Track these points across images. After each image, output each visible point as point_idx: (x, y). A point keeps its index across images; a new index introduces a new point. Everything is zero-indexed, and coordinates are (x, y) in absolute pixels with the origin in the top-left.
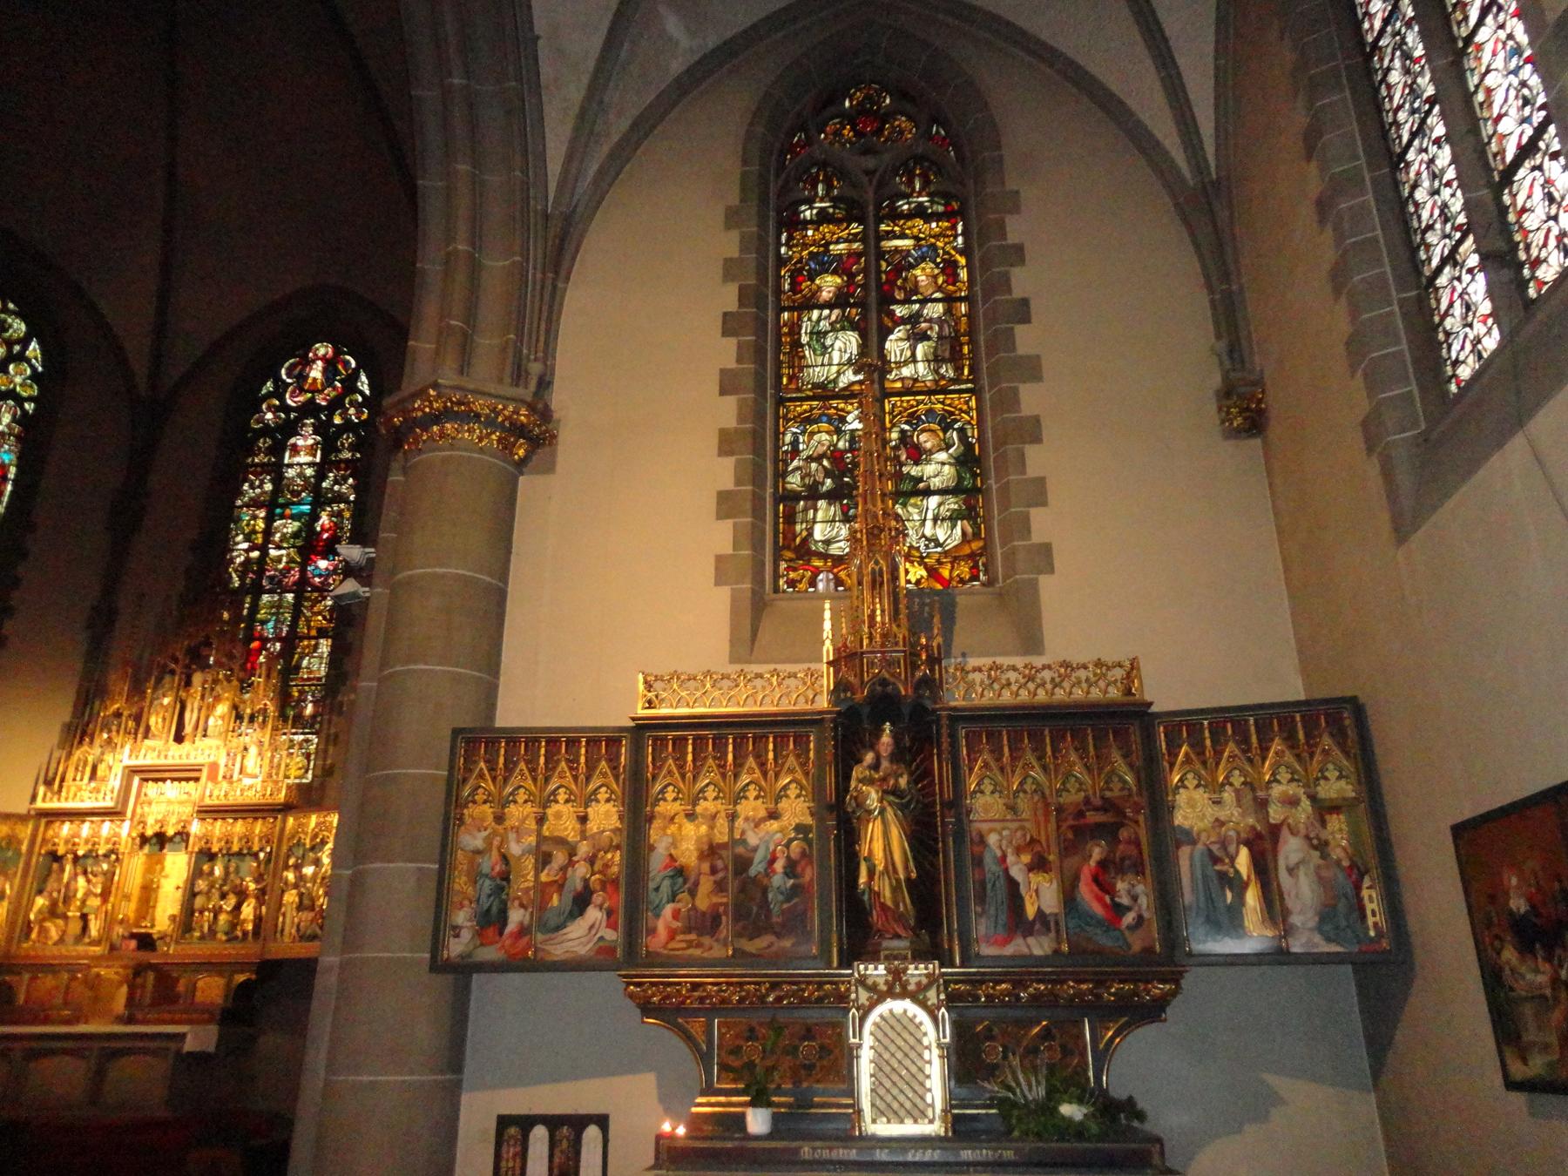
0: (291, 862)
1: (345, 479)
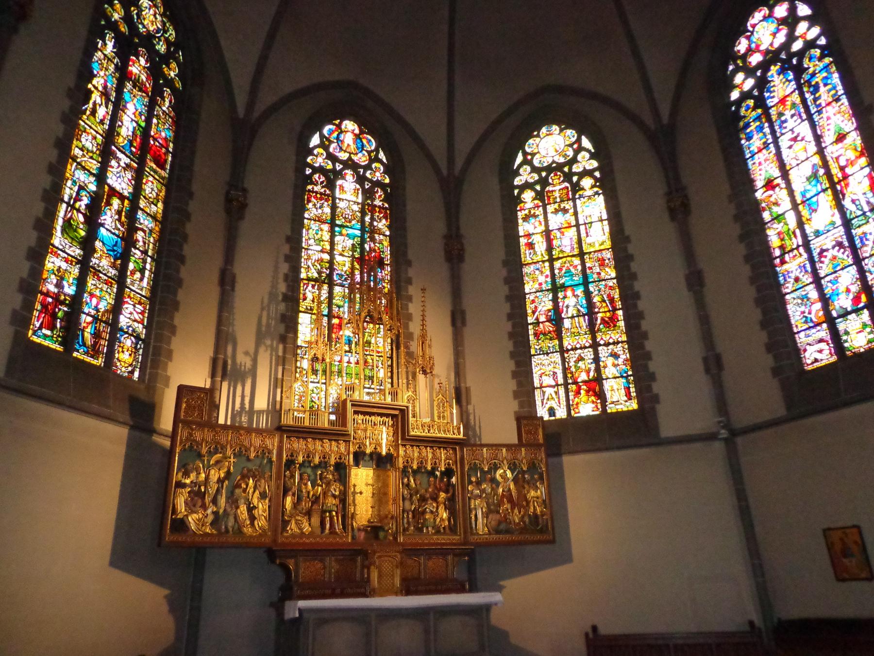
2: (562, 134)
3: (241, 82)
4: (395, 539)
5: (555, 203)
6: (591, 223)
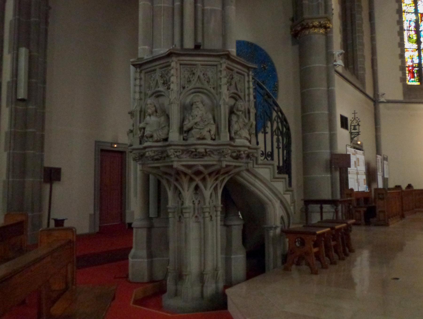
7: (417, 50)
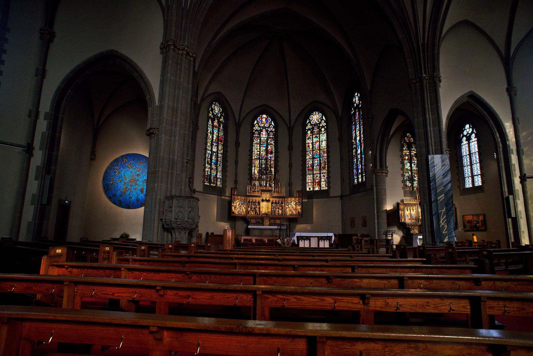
0: (287, 204)
1: (272, 141)
2: (318, 115)
3: (237, 114)
4: (270, 216)
5: (315, 135)
6: (323, 141)
7: (210, 168)
